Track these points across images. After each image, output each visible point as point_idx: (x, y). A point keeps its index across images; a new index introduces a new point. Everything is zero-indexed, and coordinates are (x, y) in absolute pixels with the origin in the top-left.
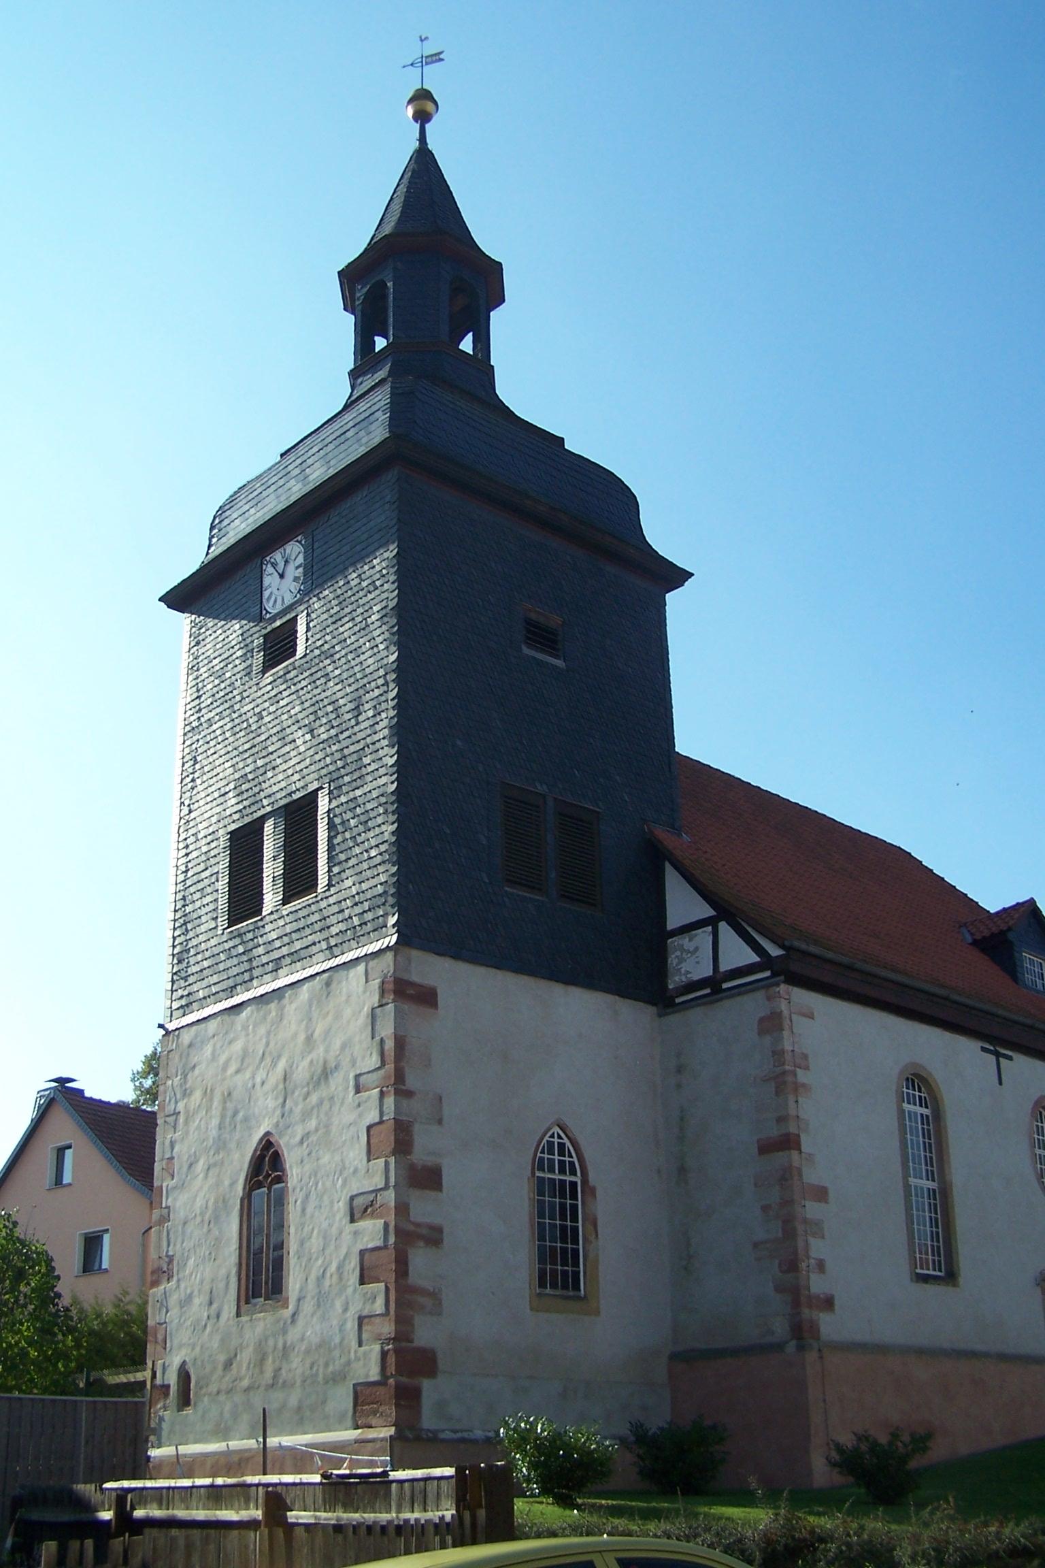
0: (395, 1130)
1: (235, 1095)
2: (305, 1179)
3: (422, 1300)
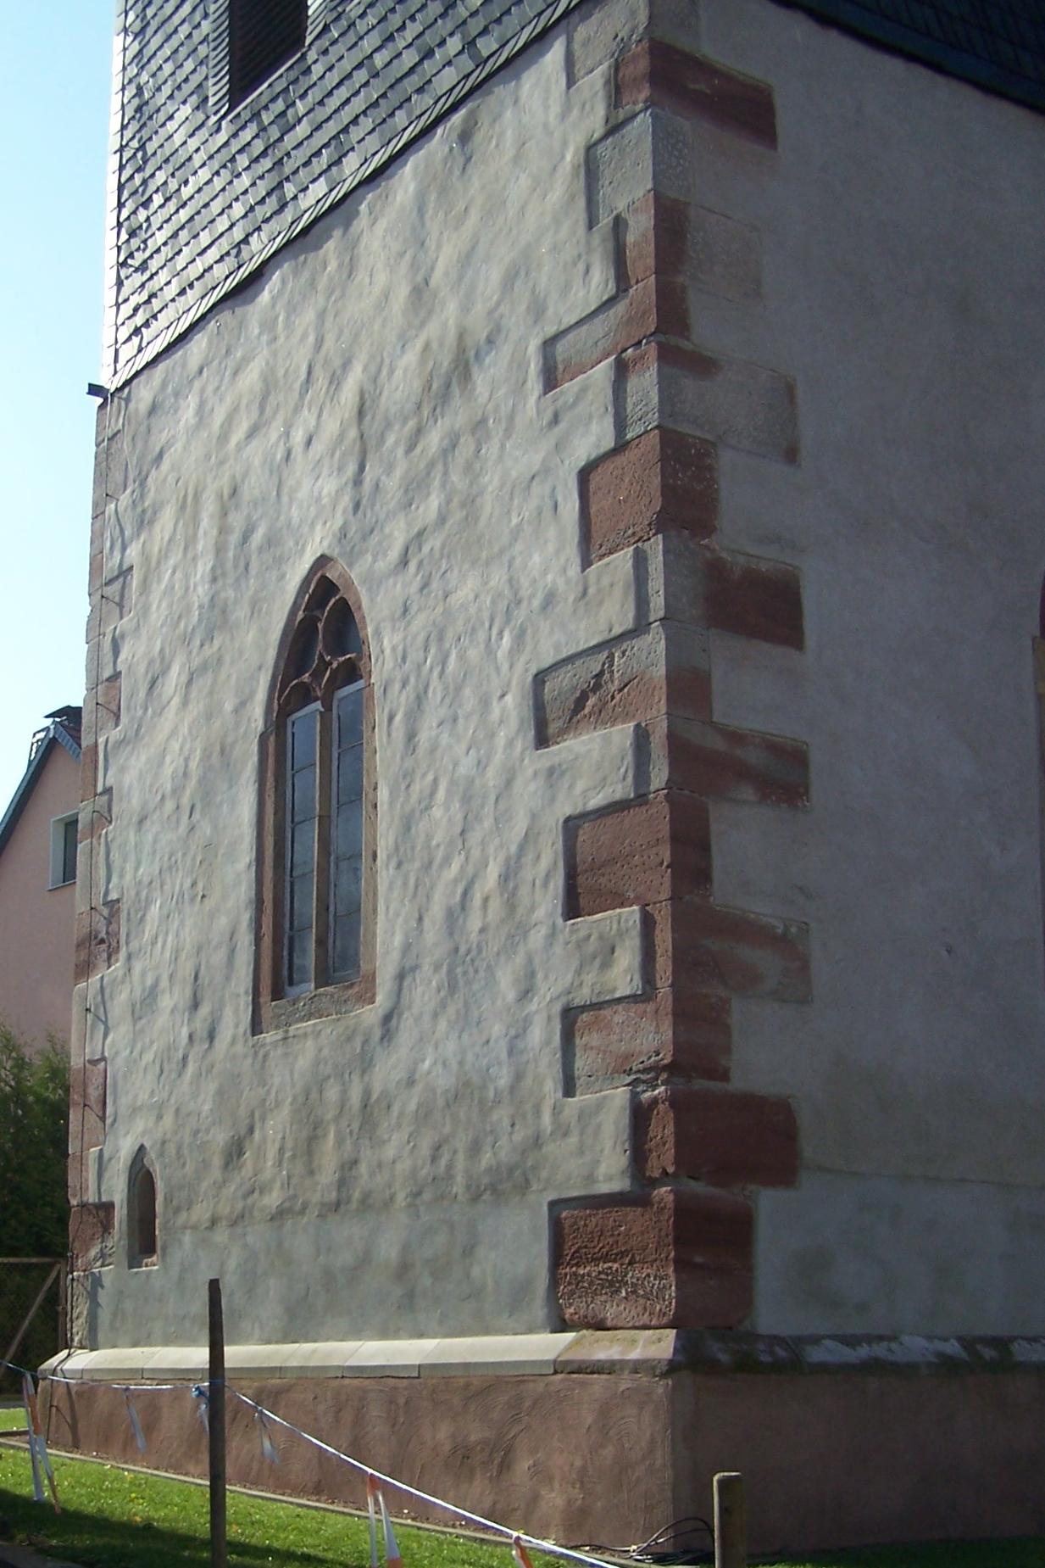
0: (664, 459)
1: (248, 492)
2: (415, 656)
3: (747, 953)
